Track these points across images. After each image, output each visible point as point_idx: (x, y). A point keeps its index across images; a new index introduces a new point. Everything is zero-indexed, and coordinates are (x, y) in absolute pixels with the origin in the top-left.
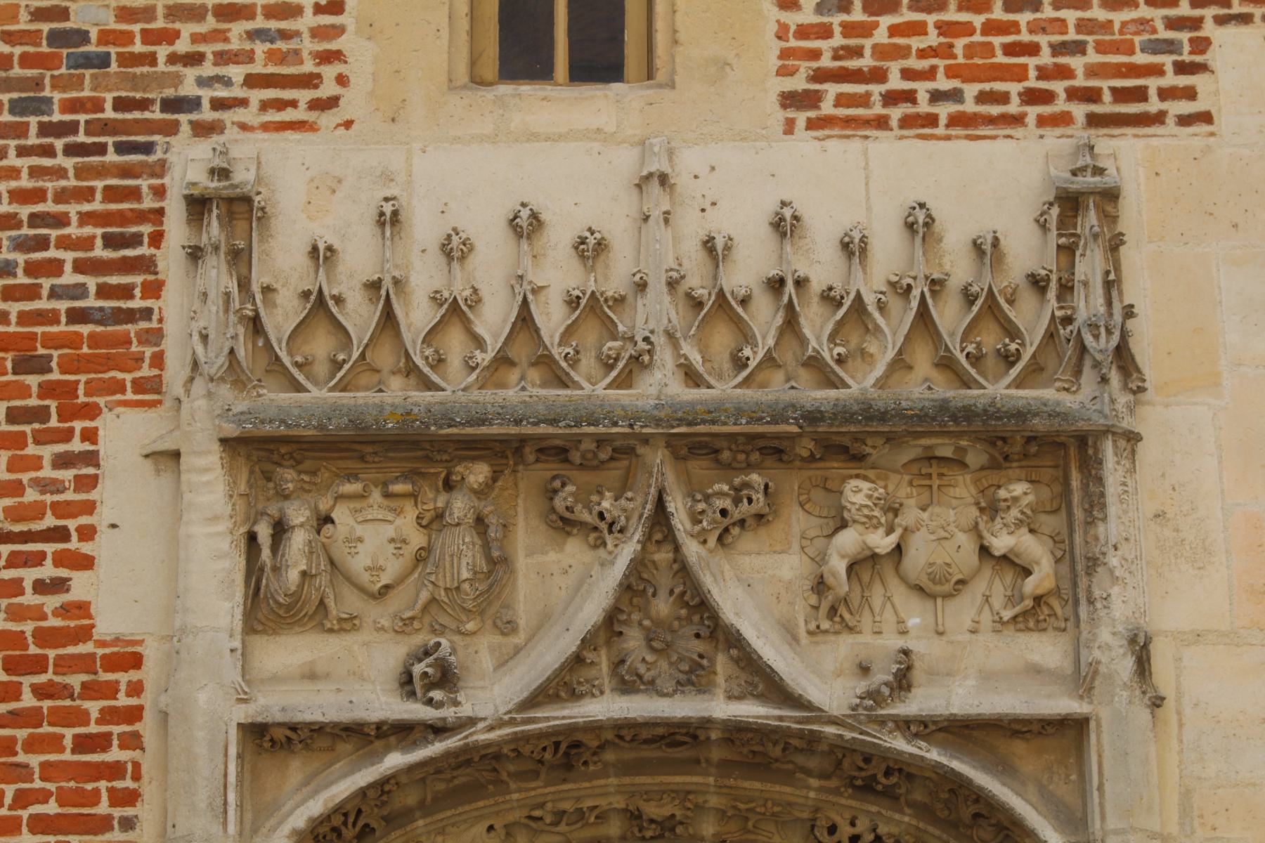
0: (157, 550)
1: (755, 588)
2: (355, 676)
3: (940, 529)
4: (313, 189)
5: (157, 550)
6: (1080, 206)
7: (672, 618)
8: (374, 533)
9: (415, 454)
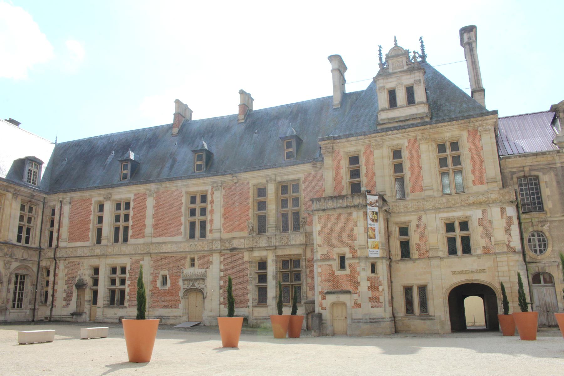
0: (181, 283)
1: (196, 284)
2: (185, 286)
3: (201, 282)
4: (185, 271)
5: (181, 283)
6: (206, 272)
7: (193, 285)
8: (186, 282)
9: (187, 280)
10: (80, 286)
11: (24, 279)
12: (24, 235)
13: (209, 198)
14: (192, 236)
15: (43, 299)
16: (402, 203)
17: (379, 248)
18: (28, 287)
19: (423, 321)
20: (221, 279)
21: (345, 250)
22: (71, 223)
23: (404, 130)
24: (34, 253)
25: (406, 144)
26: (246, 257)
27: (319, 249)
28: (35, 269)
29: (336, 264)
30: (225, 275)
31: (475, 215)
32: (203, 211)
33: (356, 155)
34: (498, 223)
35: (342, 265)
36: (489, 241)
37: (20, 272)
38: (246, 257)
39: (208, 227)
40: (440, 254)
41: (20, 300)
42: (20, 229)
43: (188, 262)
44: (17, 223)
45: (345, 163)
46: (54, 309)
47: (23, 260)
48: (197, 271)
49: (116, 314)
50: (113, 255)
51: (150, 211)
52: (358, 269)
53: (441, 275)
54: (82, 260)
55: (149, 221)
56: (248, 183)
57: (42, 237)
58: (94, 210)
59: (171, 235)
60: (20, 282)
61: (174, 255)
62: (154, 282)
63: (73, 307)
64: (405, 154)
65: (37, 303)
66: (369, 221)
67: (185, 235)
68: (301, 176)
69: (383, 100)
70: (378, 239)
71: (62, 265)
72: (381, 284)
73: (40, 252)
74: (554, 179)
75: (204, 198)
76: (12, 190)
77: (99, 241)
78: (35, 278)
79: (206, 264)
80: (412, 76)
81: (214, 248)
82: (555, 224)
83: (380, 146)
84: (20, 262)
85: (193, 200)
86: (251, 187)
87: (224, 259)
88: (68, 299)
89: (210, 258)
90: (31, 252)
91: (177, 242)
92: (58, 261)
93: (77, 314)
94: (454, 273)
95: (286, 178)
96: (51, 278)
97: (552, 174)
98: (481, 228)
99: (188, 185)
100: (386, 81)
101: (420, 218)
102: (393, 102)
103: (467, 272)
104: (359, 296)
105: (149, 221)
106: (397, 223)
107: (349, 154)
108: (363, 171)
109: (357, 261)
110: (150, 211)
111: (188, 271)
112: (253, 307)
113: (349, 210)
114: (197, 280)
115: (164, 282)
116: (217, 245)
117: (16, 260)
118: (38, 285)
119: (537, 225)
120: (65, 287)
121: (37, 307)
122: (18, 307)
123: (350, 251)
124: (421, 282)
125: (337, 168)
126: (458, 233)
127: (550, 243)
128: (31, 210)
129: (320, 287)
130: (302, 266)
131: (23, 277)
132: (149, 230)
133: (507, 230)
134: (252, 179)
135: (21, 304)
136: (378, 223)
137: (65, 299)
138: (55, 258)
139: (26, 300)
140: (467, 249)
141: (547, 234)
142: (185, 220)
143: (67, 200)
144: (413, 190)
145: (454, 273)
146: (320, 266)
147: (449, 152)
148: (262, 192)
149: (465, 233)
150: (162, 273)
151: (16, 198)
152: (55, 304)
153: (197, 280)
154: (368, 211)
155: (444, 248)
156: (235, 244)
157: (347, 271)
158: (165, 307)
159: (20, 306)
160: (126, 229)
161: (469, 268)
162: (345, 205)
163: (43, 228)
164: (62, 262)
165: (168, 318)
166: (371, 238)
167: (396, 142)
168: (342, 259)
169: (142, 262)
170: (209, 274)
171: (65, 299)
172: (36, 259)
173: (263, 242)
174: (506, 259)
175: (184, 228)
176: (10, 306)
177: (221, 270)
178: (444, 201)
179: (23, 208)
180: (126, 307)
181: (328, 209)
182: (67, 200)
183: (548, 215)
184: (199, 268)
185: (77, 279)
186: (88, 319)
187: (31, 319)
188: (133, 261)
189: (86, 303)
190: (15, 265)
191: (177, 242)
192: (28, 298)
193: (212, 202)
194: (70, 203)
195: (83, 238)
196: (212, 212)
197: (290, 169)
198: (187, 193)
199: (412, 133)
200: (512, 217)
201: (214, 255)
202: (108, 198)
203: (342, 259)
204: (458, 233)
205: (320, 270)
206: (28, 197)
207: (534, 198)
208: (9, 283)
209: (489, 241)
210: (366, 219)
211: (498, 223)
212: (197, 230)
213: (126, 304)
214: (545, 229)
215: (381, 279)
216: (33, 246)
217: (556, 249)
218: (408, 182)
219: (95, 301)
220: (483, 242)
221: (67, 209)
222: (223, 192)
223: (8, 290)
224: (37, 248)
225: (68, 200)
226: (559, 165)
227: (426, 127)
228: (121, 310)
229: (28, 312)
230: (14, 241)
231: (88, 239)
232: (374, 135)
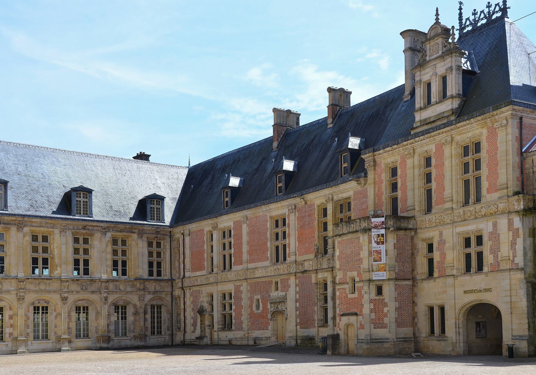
1: (279, 307)
2: (272, 309)
4: (271, 294)
8: (273, 305)
10: (201, 311)
11: (160, 308)
12: (155, 269)
16: (428, 217)
17: (385, 271)
18: (165, 315)
22: (192, 254)
24: (166, 284)
28: (169, 298)
34: (505, 236)
37: (154, 303)
42: (151, 264)
44: (146, 259)
47: (155, 292)
49: (227, 337)
50: (222, 282)
55: (245, 248)
56: (314, 204)
57: (173, 269)
58: (207, 240)
59: (261, 260)
60: (157, 311)
61: (264, 280)
62: (251, 306)
63: (198, 333)
66: (374, 245)
67: (271, 260)
70: (384, 261)
73: (172, 283)
76: (137, 231)
79: (286, 287)
90: (163, 284)
91: (264, 268)
93: (200, 338)
98: (490, 243)
99: (270, 209)
101: (441, 234)
105: (245, 248)
106: (424, 240)
111: (274, 294)
114: (280, 302)
115: (258, 307)
116: (293, 270)
117: (149, 293)
121: (174, 332)
122: (158, 334)
123: (359, 275)
126: (473, 250)
128: (159, 245)
132: (245, 257)
133: (513, 244)
135: (161, 331)
136: (384, 245)
138: (182, 288)
139: (164, 327)
143: (187, 232)
151: (141, 237)
153: (280, 302)
154: (373, 234)
159: (159, 333)
166: (375, 261)
171: (193, 325)
175: (270, 253)
176: (149, 333)
177: (297, 293)
179: (150, 244)
180: (233, 330)
181: (343, 234)
182: (187, 232)
184: (282, 291)
186: (209, 342)
187: (170, 344)
189: (207, 328)
190: (148, 297)
191: (264, 268)
194: (189, 235)
195: (201, 268)
200: (518, 229)
201: (291, 278)
204: (473, 250)
206: (153, 234)
208: (145, 313)
210: (370, 242)
211: (505, 236)
223: (145, 320)
224: (168, 280)
228: (230, 333)
229: (167, 338)
230: (146, 276)
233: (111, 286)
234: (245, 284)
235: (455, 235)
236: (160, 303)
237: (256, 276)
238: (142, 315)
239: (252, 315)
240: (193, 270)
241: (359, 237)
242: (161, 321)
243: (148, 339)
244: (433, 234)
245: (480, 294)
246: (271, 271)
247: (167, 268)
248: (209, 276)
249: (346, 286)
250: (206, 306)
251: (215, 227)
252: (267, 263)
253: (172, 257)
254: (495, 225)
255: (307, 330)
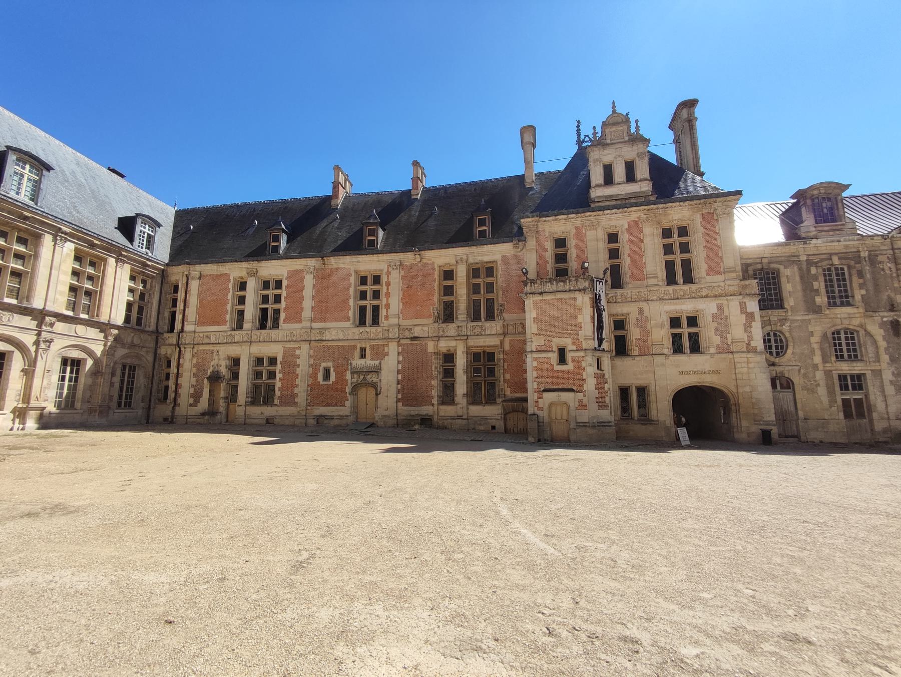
0: (348, 376)
4: (354, 363)
5: (348, 376)
6: (380, 364)
7: (364, 379)
10: (215, 378)
11: (134, 370)
13: (384, 279)
14: (362, 322)
15: (161, 395)
16: (619, 292)
18: (141, 380)
19: (644, 427)
20: (398, 372)
21: (567, 342)
22: (201, 302)
23: (625, 210)
25: (626, 226)
26: (431, 347)
27: (534, 339)
28: (150, 358)
29: (554, 357)
30: (403, 367)
31: (707, 308)
32: (376, 295)
33: (563, 236)
34: (736, 318)
35: (562, 359)
36: (724, 339)
37: (129, 361)
38: (431, 347)
39: (383, 312)
40: (666, 351)
41: (129, 397)
43: (357, 353)
45: (549, 245)
46: (177, 408)
47: (132, 346)
48: (369, 362)
51: (308, 292)
52: (583, 364)
53: (667, 375)
54: (217, 348)
55: (308, 304)
59: (336, 320)
60: (129, 374)
61: (341, 344)
62: (314, 376)
64: (624, 238)
65: (152, 401)
67: (354, 321)
68: (497, 257)
69: (597, 176)
71: (188, 354)
72: (606, 383)
74: (797, 274)
75: (377, 280)
77: (240, 326)
78: (150, 369)
80: (635, 148)
81: (391, 336)
82: (796, 324)
83: (593, 227)
84: (129, 348)
85: (363, 280)
86: (437, 269)
87: (403, 349)
88: (197, 396)
89: (386, 349)
90: (144, 336)
91: (342, 330)
92: (182, 349)
94: (681, 373)
95: (479, 259)
96: (173, 369)
97: (796, 267)
98: (715, 324)
100: (602, 152)
102: (609, 180)
103: (697, 373)
104: (585, 395)
105: (308, 304)
107: (555, 236)
108: (572, 255)
109: (582, 354)
110: (308, 292)
111: (358, 363)
112: (438, 404)
113: (572, 295)
117: (123, 345)
118: (155, 378)
119: (775, 324)
120: (193, 381)
121: (152, 405)
122: (125, 406)
123: (574, 343)
124: (641, 383)
125: (540, 251)
126: (685, 330)
127: (791, 344)
129: (535, 383)
130: (499, 360)
131: (133, 368)
132: (307, 313)
133: (747, 327)
134: (441, 257)
135: (130, 402)
137: (192, 396)
138: (178, 345)
140: (696, 348)
141: (787, 335)
142: (353, 303)
144: (633, 279)
145: (681, 373)
146: (536, 359)
147: (676, 240)
148: (448, 275)
149: (693, 330)
150: (324, 365)
152: (178, 401)
155: (668, 343)
156: (417, 332)
157: (570, 366)
158: (328, 405)
159: (128, 405)
160: (277, 312)
161: (699, 368)
162: (567, 288)
163: (161, 307)
164: (188, 350)
165: (332, 418)
167: (613, 223)
168: (562, 352)
169: (297, 352)
170: (383, 366)
171: (192, 396)
172: (153, 345)
173: (451, 329)
174: (746, 360)
176: (114, 404)
177: (399, 362)
178: (671, 292)
183: (789, 314)
184: (372, 359)
185: (210, 371)
186: (224, 420)
188: (286, 350)
189: (222, 401)
191: (342, 330)
192: (140, 394)
193: (388, 284)
194: (200, 279)
196: (388, 295)
197: (486, 248)
198: (356, 272)
199: (635, 214)
202: (253, 274)
203: (562, 352)
205: (535, 364)
207: (771, 295)
208: (113, 374)
209: (724, 339)
211: (736, 318)
212: (368, 316)
213: (276, 402)
214: (785, 328)
215: (606, 377)
216: (147, 329)
217: (797, 351)
218: (627, 269)
219: (232, 397)
220: (717, 340)
221: (194, 285)
222: (402, 272)
223: (112, 385)
225: (197, 274)
226: (803, 258)
227: (652, 206)
229: (140, 412)
231: (225, 323)
232: (589, 214)
233: (60, 327)
234: (305, 347)
235: (662, 313)
236: (135, 362)
237: (327, 338)
238: (107, 377)
239: (313, 387)
240: (200, 322)
241: (575, 298)
242: (132, 389)
243: (111, 412)
244: (621, 309)
245: (703, 376)
246: (356, 332)
247: (153, 316)
248: (233, 333)
249: (550, 355)
250: (224, 371)
251: (253, 274)
252: (347, 324)
253: (162, 304)
254: (720, 307)
255: (417, 408)
